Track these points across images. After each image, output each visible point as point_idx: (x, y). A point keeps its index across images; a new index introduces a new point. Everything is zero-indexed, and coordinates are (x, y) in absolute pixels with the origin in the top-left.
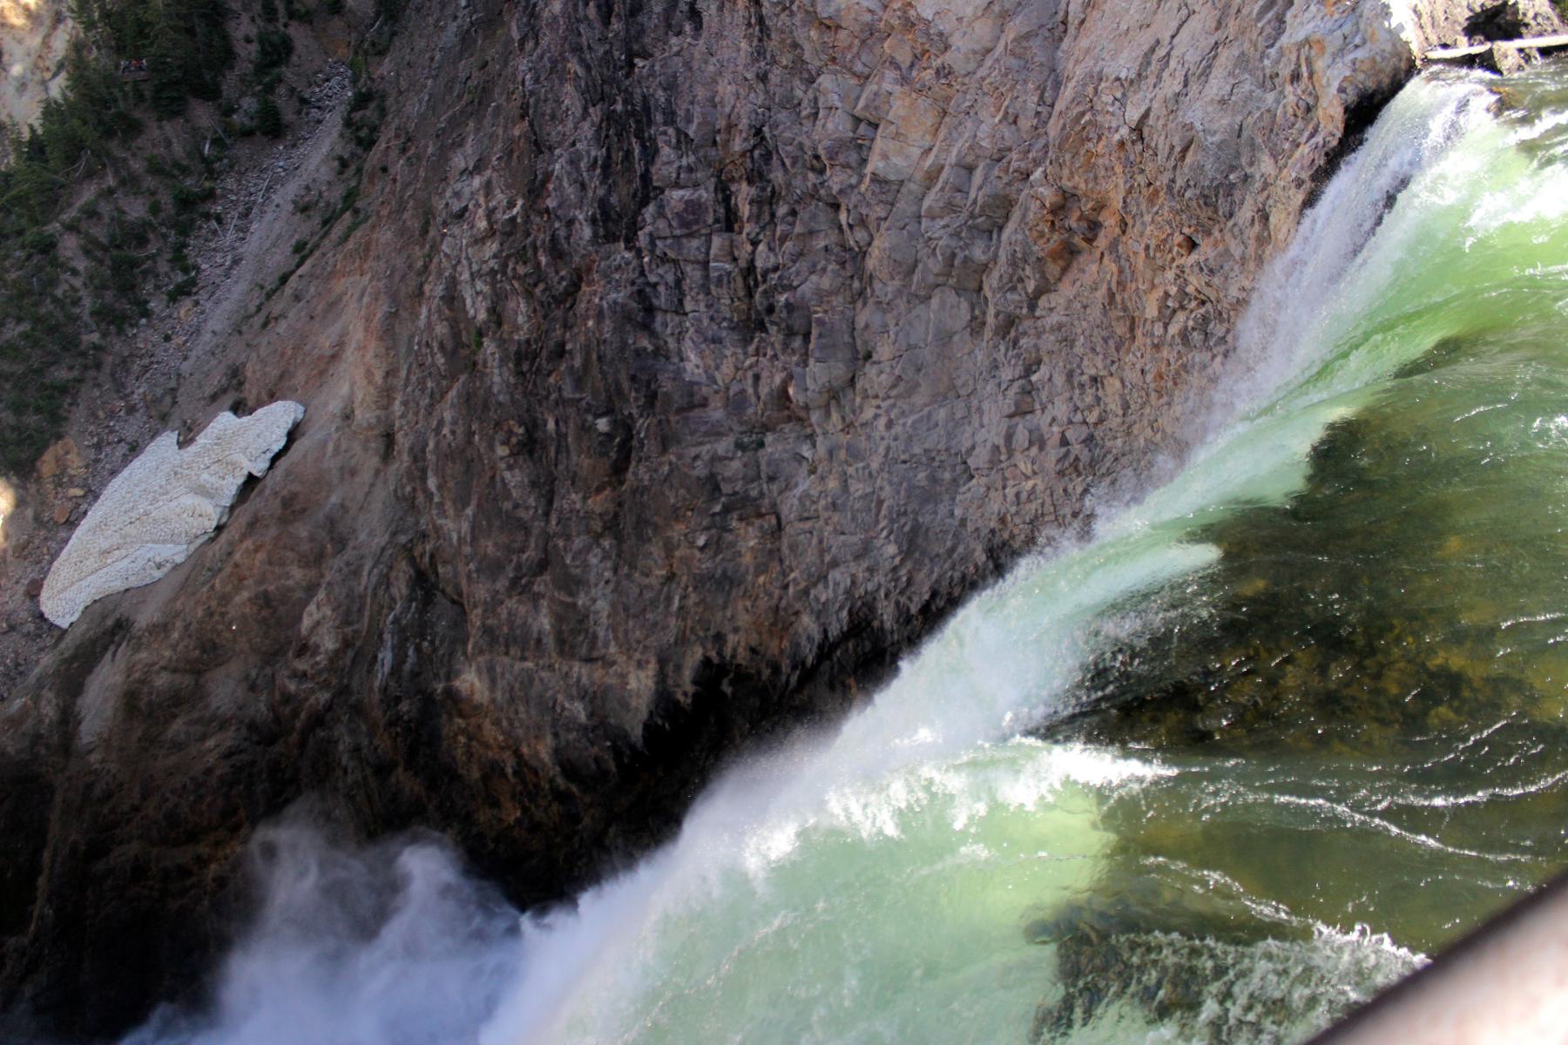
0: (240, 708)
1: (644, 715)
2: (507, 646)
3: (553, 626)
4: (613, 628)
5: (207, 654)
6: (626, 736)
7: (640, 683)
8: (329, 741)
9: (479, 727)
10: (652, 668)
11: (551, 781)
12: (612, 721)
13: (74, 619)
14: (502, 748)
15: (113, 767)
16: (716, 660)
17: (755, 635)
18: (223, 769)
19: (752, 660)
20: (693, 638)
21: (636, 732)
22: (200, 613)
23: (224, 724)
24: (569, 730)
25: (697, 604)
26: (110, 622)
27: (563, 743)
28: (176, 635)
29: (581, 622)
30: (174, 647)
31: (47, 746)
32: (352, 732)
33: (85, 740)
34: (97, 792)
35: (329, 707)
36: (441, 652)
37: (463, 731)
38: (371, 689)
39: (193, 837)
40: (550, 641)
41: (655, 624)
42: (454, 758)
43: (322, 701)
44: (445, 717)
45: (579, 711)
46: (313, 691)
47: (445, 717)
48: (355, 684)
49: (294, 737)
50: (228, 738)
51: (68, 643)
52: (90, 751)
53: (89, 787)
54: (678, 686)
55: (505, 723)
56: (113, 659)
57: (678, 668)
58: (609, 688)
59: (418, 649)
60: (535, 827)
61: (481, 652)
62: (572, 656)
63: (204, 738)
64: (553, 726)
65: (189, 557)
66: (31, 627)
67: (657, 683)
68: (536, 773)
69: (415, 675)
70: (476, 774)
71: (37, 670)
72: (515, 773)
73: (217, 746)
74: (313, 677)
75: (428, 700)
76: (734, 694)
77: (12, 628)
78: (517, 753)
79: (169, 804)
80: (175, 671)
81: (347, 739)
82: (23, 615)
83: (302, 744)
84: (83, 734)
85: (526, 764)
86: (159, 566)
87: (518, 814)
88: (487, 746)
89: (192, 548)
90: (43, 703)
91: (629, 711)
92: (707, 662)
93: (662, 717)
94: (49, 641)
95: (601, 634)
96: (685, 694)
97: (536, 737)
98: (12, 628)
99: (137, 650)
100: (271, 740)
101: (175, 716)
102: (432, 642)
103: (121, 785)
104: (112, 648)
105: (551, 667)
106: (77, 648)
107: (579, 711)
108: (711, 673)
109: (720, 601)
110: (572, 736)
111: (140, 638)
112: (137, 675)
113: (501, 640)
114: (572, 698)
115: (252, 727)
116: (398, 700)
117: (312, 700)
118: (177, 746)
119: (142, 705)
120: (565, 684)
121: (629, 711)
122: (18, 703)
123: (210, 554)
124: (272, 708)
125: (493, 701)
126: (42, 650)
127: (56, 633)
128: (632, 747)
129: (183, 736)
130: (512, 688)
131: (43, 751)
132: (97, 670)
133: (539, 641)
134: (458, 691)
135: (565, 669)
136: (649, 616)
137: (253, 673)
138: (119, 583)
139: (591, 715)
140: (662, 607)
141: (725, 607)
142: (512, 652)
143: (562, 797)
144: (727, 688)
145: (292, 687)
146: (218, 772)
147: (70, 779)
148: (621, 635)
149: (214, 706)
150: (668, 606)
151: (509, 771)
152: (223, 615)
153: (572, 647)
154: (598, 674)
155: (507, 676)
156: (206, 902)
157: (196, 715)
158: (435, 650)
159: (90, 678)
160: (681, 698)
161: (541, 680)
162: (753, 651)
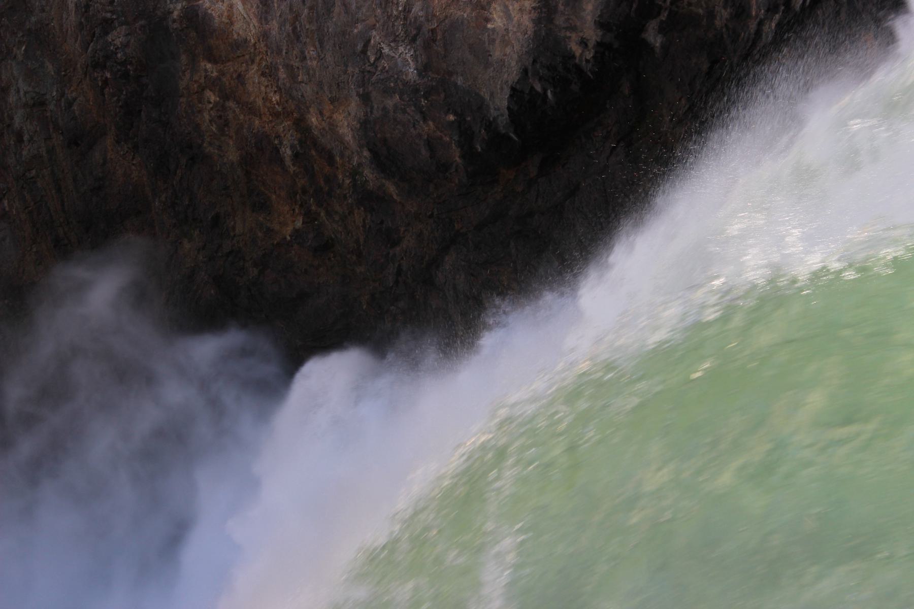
1: (512, 74)
11: (355, 173)
12: (460, 81)
14: (276, 115)
21: (499, 103)
27: (377, 114)
44: (184, 58)
45: (406, 60)
54: (573, 28)
55: (282, 74)
60: (325, 247)
64: (363, 83)
67: (537, 22)
68: (330, 159)
70: (233, 155)
72: (296, 156)
78: (301, 125)
81: (23, 86)
87: (299, 224)
88: (251, 110)
91: (487, 65)
93: (541, 79)
96: (583, 43)
97: (332, 101)
110: (389, 103)
116: (107, 26)
121: (487, 65)
125: (265, 35)
128: (490, 125)
130: (297, 17)
134: (207, 17)
139: (424, 70)
143: (370, 200)
144: (654, 38)
151: (287, 152)
160: (577, 50)
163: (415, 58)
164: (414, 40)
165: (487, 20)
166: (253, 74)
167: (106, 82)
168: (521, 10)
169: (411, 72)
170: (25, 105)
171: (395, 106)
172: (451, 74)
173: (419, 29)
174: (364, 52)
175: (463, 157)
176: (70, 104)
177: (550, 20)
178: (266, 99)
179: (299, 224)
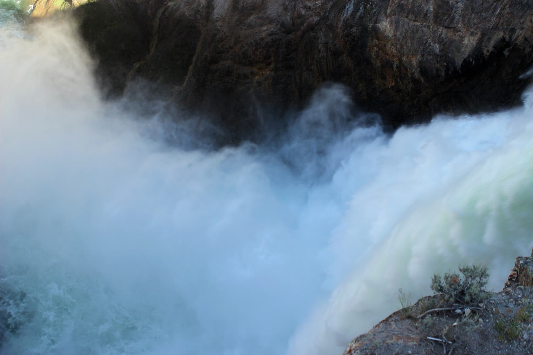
0: (279, 16)
1: (465, 56)
2: (408, 14)
3: (434, 9)
4: (463, 16)
6: (454, 62)
7: (469, 42)
8: (315, 38)
9: (385, 45)
10: (477, 37)
11: (413, 74)
12: (450, 55)
14: (394, 56)
15: (225, 30)
16: (507, 40)
17: (530, 33)
18: (269, 39)
19: (523, 43)
20: (501, 28)
21: (459, 62)
23: (271, 22)
24: (430, 55)
25: (508, 13)
27: (425, 60)
29: (448, 10)
31: (201, 16)
32: (325, 36)
33: (215, 17)
34: (218, 38)
35: (318, 24)
36: (374, 11)
37: (376, 45)
38: (339, 20)
39: (251, 64)
40: (431, 16)
41: (485, 19)
42: (371, 56)
43: (315, 20)
44: (370, 38)
45: (437, 48)
46: (312, 16)
47: (370, 38)
48: (331, 17)
49: (299, 33)
50: (272, 28)
52: (218, 21)
53: (215, 35)
54: (486, 47)
55: (398, 46)
57: (489, 39)
58: (453, 41)
59: (365, 7)
60: (399, 91)
61: (395, 14)
62: (440, 24)
63: (262, 25)
64: (423, 51)
67: (477, 43)
68: (406, 70)
69: (361, 18)
70: (379, 64)
72: (397, 67)
73: (267, 30)
74: (313, 9)
75: (365, 29)
76: (508, 55)
78: (400, 60)
79: (245, 49)
83: (302, 36)
84: (215, 14)
85: (403, 65)
87: (393, 84)
88: (387, 54)
91: (459, 52)
92: (503, 40)
95: (457, 17)
96: (488, 51)
100: (289, 32)
101: (251, 14)
102: (371, 5)
103: (227, 37)
105: (428, 27)
107: (437, 48)
108: (503, 44)
109: (520, 15)
110: (429, 58)
113: (406, 11)
114: (435, 42)
115: (283, 25)
116: (352, 26)
117: (311, 19)
118: (250, 26)
119: (240, 7)
120: (433, 36)
121: (459, 52)
124: (292, 19)
128: (455, 68)
129: (254, 23)
130: (407, 32)
131: (199, 17)
133: (426, 15)
134: (379, 29)
135: (436, 29)
136: (484, 14)
137: (287, 3)
140: (490, 11)
141: (521, 17)
142: (410, 17)
143: (415, 81)
144: (506, 53)
145: (303, 12)
146: (266, 40)
147: (207, 30)
148: (466, 20)
149: (268, 13)
150: (493, 12)
151: (395, 66)
153: (441, 20)
154: (450, 34)
155: (406, 27)
156: (252, 90)
157: (260, 15)
158: (372, 9)
160: (485, 52)
161: (423, 31)
162: (526, 39)
163: (439, 47)
164: (440, 43)
165: (463, 41)
166: (389, 45)
167: (348, 41)
168: (474, 40)
169: (438, 51)
170: (323, 43)
171: (430, 59)
172: (448, 53)
173: (443, 40)
174: (426, 44)
175: (445, 74)
176: (336, 45)
177: (481, 43)
178: (392, 52)
179: (393, 84)
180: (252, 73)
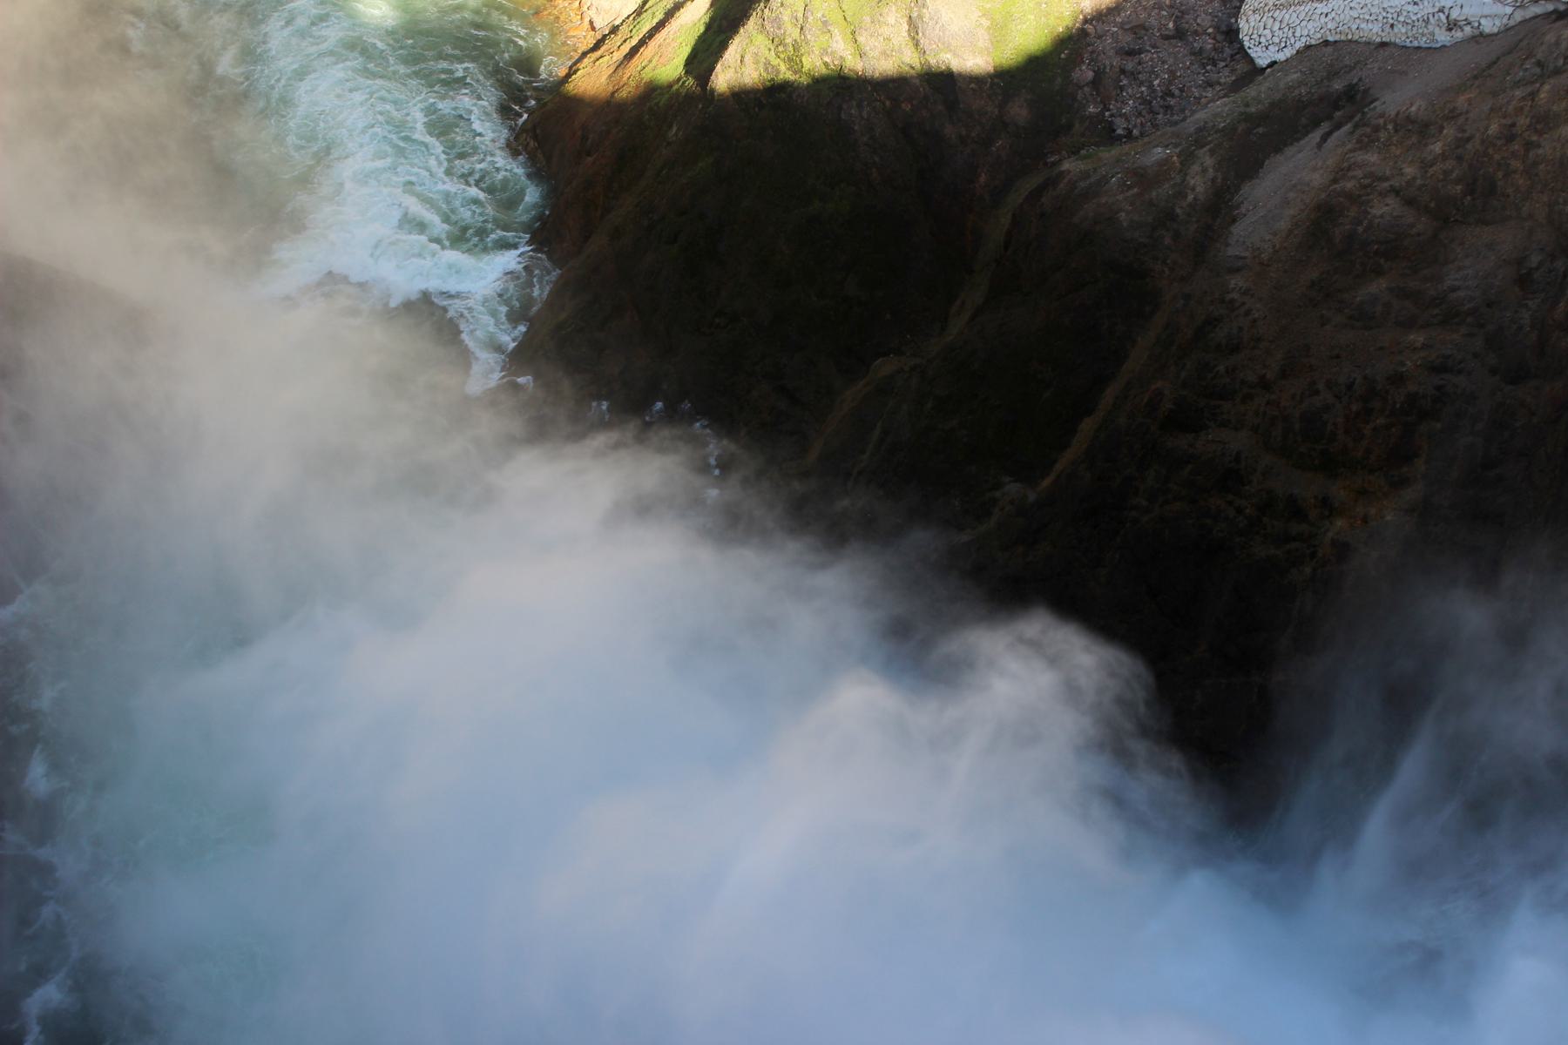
5: (1474, 195)
13: (1281, 57)
22: (1494, 128)
26: (1338, 85)
28: (1437, 148)
30: (1425, 165)
33: (1231, 252)
51: (1258, 92)
52: (1238, 270)
56: (1319, 146)
65: (1508, 29)
66: (1209, 44)
71: (1201, 115)
73: (1425, 346)
77: (1180, 34)
80: (1410, 202)
82: (1205, 20)
86: (1452, 26)
89: (1519, 16)
90: (1196, 168)
94: (1226, 77)
98: (1180, 34)
99: (1363, 145)
101: (1378, 272)
104: (1325, 126)
106: (1272, 104)
111: (1377, 129)
112: (1349, 185)
122: (1159, 152)
123: (1550, 38)
126: (1210, 84)
127: (1241, 67)
131: (1167, 241)
132: (1290, 151)
137: (1535, 260)
138: (1376, 28)
152: (1529, 146)
159: (1280, 158)
180: (1325, 502)
